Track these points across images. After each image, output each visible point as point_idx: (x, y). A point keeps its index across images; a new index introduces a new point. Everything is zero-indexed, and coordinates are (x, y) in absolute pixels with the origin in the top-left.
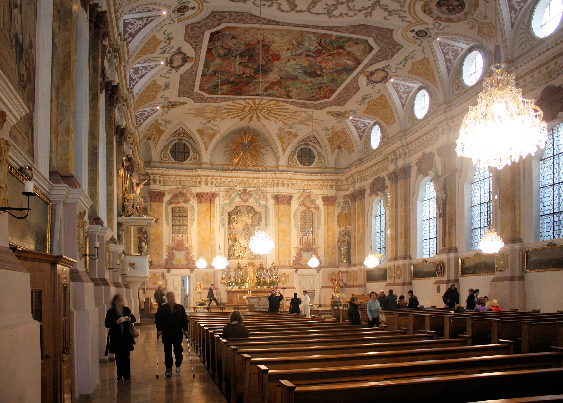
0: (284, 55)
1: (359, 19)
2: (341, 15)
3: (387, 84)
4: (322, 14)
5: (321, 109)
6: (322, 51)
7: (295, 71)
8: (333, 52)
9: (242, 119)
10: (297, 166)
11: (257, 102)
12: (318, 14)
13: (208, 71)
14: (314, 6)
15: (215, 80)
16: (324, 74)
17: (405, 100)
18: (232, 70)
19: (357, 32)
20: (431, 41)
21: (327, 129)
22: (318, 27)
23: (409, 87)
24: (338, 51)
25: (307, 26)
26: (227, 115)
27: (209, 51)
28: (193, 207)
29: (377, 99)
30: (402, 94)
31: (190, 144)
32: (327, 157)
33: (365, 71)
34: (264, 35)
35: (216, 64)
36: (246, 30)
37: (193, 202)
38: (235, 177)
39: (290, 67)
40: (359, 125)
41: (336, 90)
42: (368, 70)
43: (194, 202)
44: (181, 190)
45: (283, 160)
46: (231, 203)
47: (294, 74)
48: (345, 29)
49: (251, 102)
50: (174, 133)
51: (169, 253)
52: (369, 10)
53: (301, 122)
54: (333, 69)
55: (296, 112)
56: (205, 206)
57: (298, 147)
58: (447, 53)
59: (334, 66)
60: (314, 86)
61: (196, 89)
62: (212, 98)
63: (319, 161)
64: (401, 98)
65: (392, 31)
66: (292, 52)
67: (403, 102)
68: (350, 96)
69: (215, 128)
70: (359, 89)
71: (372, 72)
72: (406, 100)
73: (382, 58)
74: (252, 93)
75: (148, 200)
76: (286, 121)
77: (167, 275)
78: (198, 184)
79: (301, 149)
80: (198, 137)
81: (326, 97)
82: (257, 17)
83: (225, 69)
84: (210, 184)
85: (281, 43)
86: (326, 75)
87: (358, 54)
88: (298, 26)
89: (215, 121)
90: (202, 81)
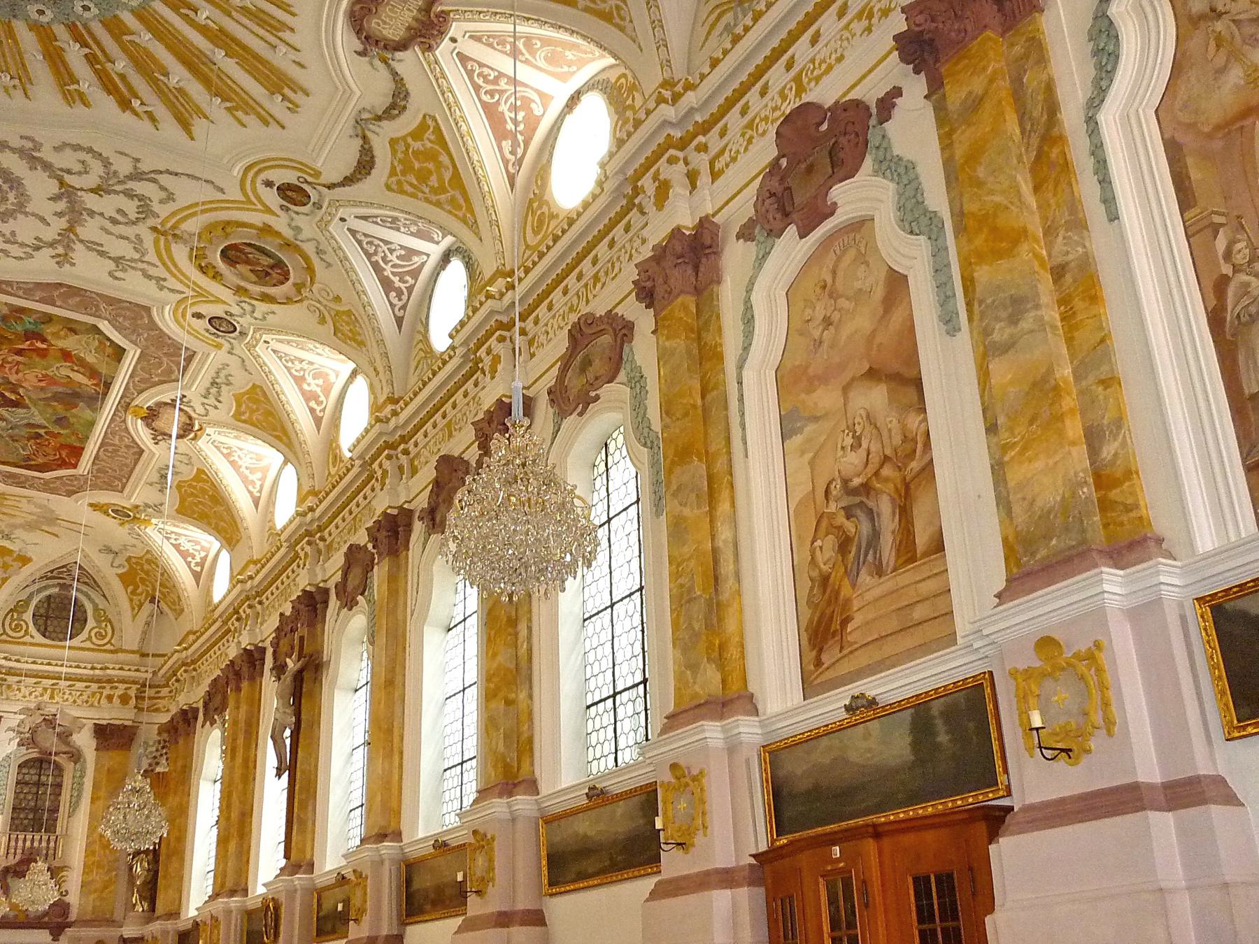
1: (42, 268)
3: (202, 443)
5: (70, 494)
8: (20, 347)
10: (27, 639)
16: (27, 401)
19: (58, 303)
21: (108, 550)
23: (259, 459)
24: (32, 344)
29: (192, 480)
30: (247, 472)
32: (120, 621)
33: (133, 404)
40: (187, 546)
41: (83, 449)
42: (136, 402)
48: (20, 288)
52: (60, 250)
53: (31, 527)
54: (42, 389)
57: (39, 591)
58: (303, 378)
59: (43, 384)
60: (17, 431)
63: (97, 630)
64: (245, 481)
67: (255, 491)
68: (126, 465)
70: (143, 451)
72: (262, 486)
73: (157, 375)
79: (49, 597)
81: (63, 464)
87: (90, 359)
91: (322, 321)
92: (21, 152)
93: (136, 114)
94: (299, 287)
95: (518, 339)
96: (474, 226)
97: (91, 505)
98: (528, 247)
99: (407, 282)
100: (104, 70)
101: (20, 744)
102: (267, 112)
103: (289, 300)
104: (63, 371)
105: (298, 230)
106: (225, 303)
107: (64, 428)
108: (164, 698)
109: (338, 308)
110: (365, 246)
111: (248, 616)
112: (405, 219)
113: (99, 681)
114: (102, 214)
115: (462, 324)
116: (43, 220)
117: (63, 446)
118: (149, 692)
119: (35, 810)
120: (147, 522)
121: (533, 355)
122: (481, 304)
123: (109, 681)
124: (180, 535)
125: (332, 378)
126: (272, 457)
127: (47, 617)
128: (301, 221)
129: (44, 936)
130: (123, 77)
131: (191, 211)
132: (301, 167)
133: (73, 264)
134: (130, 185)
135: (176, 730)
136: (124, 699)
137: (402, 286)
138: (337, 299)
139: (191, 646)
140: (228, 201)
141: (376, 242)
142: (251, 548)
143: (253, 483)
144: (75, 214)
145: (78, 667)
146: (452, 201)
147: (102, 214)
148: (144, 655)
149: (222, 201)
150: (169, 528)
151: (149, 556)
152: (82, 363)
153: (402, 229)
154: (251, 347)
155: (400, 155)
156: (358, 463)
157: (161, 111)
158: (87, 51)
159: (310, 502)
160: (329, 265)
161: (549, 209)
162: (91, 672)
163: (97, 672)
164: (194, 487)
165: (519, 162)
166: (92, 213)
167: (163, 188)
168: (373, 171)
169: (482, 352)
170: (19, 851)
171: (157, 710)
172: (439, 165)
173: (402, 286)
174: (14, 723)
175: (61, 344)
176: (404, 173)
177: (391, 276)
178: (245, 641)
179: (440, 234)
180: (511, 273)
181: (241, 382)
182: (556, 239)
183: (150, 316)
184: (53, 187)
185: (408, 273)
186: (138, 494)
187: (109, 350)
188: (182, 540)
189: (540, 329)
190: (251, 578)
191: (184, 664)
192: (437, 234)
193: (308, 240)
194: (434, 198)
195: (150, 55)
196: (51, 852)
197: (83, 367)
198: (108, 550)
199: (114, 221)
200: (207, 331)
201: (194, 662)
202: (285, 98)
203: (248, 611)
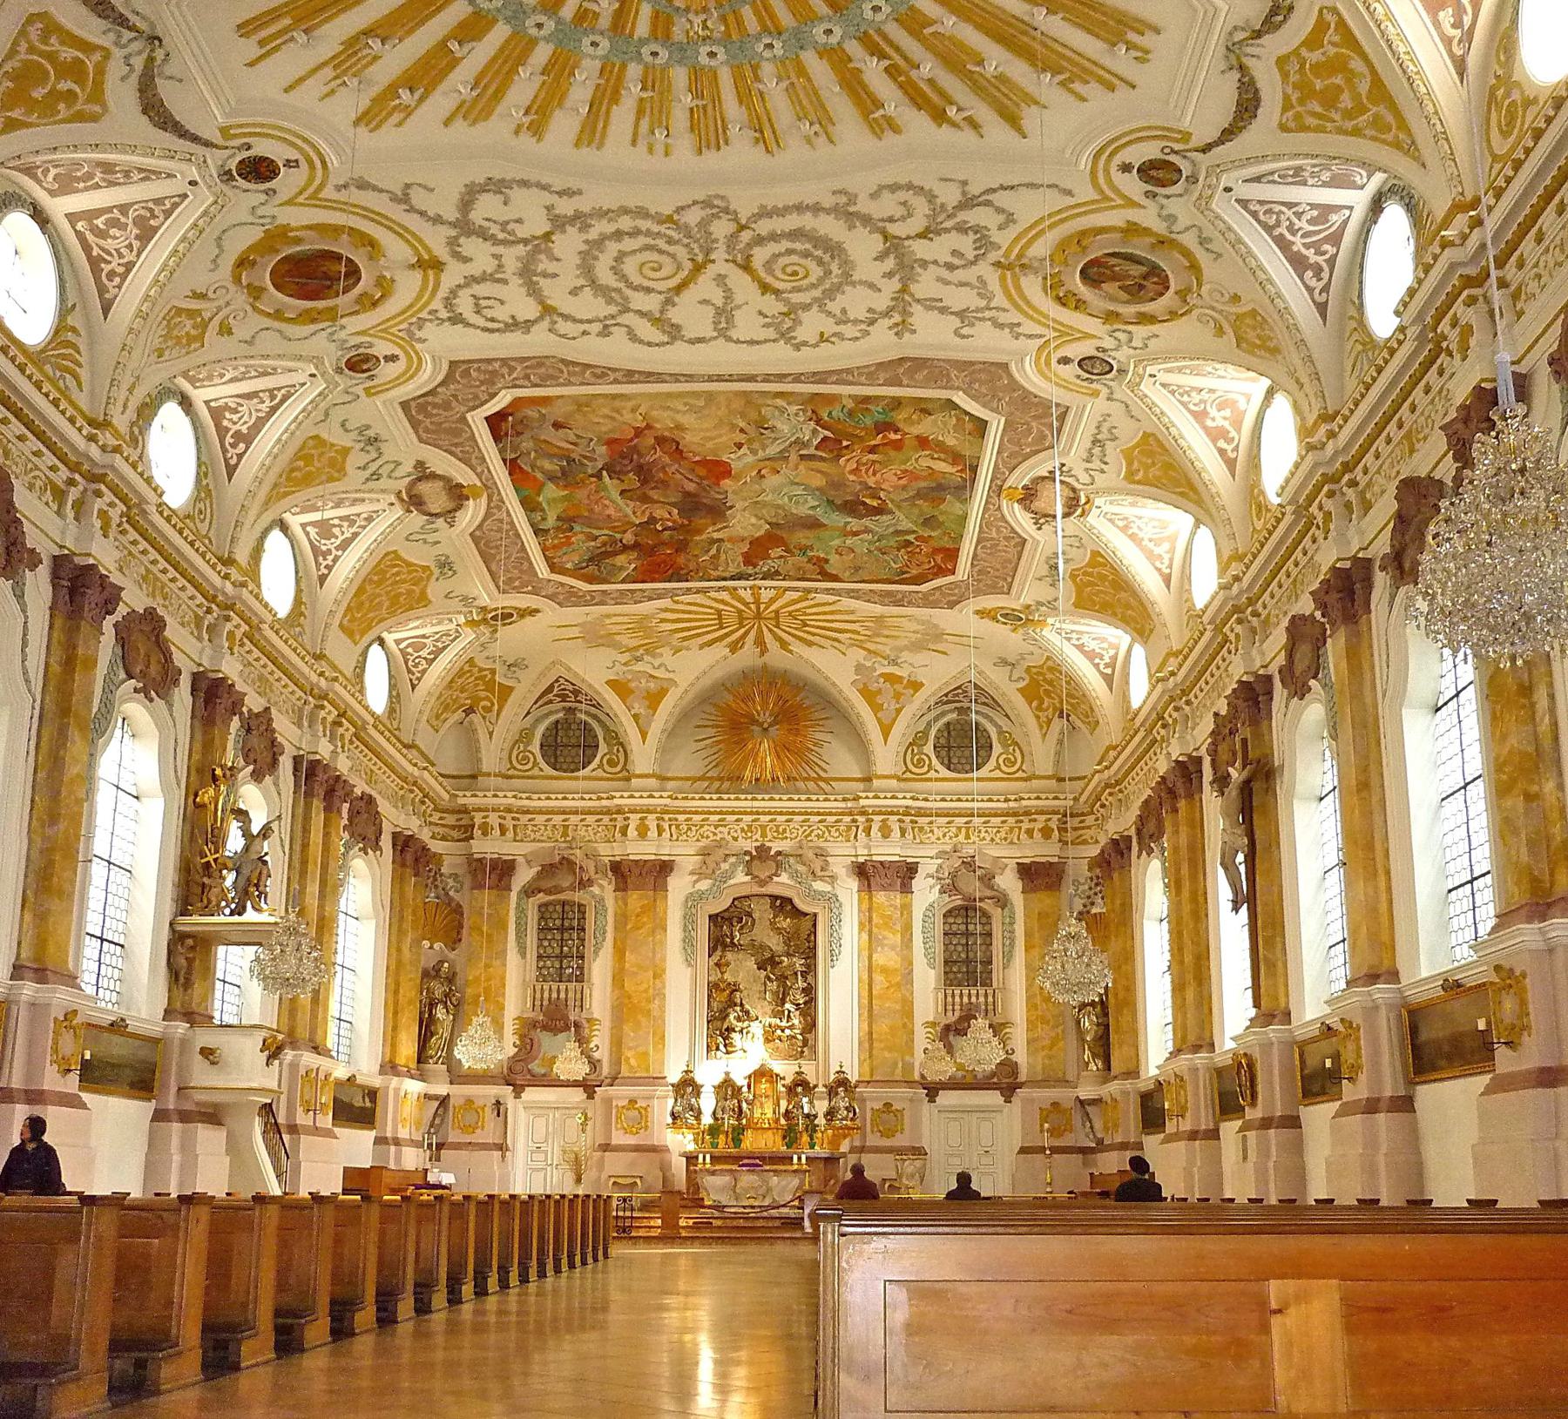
0: (741, 461)
1: (882, 343)
2: (823, 338)
3: (1092, 519)
4: (766, 341)
5: (951, 605)
6: (840, 442)
7: (797, 503)
9: (734, 648)
10: (932, 774)
11: (747, 595)
12: (758, 343)
13: (544, 519)
14: (730, 320)
15: (581, 545)
17: (1167, 562)
18: (611, 511)
19: (905, 382)
20: (1139, 384)
21: (1004, 662)
22: (781, 377)
25: (751, 378)
26: (685, 639)
27: (513, 467)
28: (601, 901)
30: (1151, 545)
31: (599, 721)
32: (1029, 744)
34: (642, 410)
35: (554, 500)
36: (582, 404)
37: (601, 887)
38: (733, 813)
39: (777, 490)
40: (1092, 645)
43: (605, 889)
44: (566, 853)
45: (886, 757)
46: (717, 891)
47: (803, 511)
49: (725, 595)
50: (550, 689)
51: (522, 1037)
52: (897, 318)
53: (917, 647)
54: (904, 488)
55: (879, 619)
56: (635, 899)
57: (936, 719)
59: (903, 482)
61: (542, 570)
62: (604, 592)
64: (1151, 557)
65: (1005, 366)
66: (754, 452)
68: (1010, 562)
69: (659, 673)
71: (1025, 488)
72: (1171, 560)
73: (1029, 445)
74: (714, 574)
75: (467, 886)
76: (868, 645)
77: (510, 1102)
78: (618, 835)
80: (612, 699)
81: (940, 572)
82: (588, 366)
83: (591, 511)
84: (653, 833)
85: (707, 430)
86: (899, 507)
87: (951, 441)
88: (720, 379)
89: (654, 656)
90: (544, 550)
91: (1220, 331)
92: (835, 211)
93: (954, 125)
94: (1183, 294)
95: (1497, 296)
96: (1410, 148)
97: (977, 612)
98: (1495, 158)
99: (1324, 253)
100: (910, 82)
101: (942, 892)
102: (1109, 72)
103: (1173, 315)
104: (924, 461)
105: (1171, 219)
106: (1094, 337)
107: (933, 530)
108: (1089, 828)
109: (1240, 310)
110: (1262, 217)
111: (1175, 721)
112: (1314, 166)
113: (1015, 814)
114: (935, 262)
115: (1411, 292)
116: (872, 286)
117: (936, 551)
118: (1072, 823)
119: (968, 961)
120: (1042, 623)
121: (1520, 314)
122: (1436, 258)
123: (1027, 813)
124: (1082, 633)
125: (1242, 405)
126: (1178, 520)
127: (949, 748)
128: (1173, 206)
129: (994, 1098)
130: (931, 82)
131: (1036, 230)
132: (1164, 133)
133: (914, 332)
134: (962, 216)
135: (1109, 863)
136: (1046, 833)
137: (1320, 259)
138: (1236, 298)
139: (1112, 763)
140: (1078, 205)
141: (1277, 208)
142: (1168, 637)
143: (1160, 557)
144: (906, 269)
145: (990, 800)
146: (1376, 121)
147: (935, 262)
148: (1063, 780)
149: (1073, 207)
150: (1068, 627)
151: (1050, 663)
152: (941, 447)
153: (1310, 182)
154: (1134, 386)
155: (1294, 78)
156: (1289, 509)
157: (983, 113)
158: (887, 63)
159: (1235, 569)
160: (1219, 255)
161: (1522, 93)
162: (1005, 805)
163: (1012, 804)
164: (1091, 575)
165: (1469, 35)
166: (924, 264)
167: (999, 210)
168: (1260, 111)
169: (1444, 327)
170: (957, 1007)
171: (1085, 842)
172: (1350, 76)
173: (1320, 259)
174: (932, 869)
175: (916, 430)
176: (1301, 101)
177: (1304, 251)
178: (1176, 751)
179: (1364, 174)
180: (1475, 204)
181: (1128, 434)
182: (1538, 135)
183: (1010, 376)
184: (876, 243)
185: (1326, 240)
186: (1027, 592)
187: (969, 426)
188: (1085, 639)
189: (1528, 272)
190: (1173, 674)
191: (1108, 786)
192: (1360, 175)
193: (1187, 229)
194: (1349, 125)
195: (961, 46)
196: (990, 1007)
197: (945, 452)
198: (1004, 662)
199: (950, 267)
200: (1078, 377)
201: (1118, 783)
202: (1130, 47)
203: (1175, 715)
